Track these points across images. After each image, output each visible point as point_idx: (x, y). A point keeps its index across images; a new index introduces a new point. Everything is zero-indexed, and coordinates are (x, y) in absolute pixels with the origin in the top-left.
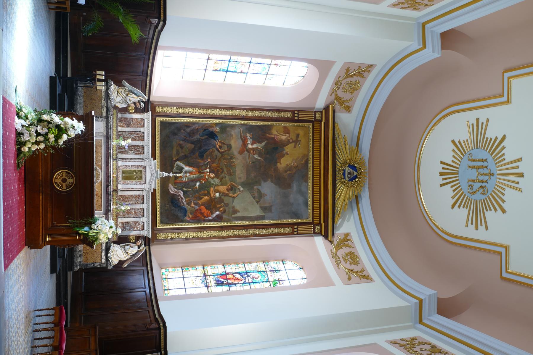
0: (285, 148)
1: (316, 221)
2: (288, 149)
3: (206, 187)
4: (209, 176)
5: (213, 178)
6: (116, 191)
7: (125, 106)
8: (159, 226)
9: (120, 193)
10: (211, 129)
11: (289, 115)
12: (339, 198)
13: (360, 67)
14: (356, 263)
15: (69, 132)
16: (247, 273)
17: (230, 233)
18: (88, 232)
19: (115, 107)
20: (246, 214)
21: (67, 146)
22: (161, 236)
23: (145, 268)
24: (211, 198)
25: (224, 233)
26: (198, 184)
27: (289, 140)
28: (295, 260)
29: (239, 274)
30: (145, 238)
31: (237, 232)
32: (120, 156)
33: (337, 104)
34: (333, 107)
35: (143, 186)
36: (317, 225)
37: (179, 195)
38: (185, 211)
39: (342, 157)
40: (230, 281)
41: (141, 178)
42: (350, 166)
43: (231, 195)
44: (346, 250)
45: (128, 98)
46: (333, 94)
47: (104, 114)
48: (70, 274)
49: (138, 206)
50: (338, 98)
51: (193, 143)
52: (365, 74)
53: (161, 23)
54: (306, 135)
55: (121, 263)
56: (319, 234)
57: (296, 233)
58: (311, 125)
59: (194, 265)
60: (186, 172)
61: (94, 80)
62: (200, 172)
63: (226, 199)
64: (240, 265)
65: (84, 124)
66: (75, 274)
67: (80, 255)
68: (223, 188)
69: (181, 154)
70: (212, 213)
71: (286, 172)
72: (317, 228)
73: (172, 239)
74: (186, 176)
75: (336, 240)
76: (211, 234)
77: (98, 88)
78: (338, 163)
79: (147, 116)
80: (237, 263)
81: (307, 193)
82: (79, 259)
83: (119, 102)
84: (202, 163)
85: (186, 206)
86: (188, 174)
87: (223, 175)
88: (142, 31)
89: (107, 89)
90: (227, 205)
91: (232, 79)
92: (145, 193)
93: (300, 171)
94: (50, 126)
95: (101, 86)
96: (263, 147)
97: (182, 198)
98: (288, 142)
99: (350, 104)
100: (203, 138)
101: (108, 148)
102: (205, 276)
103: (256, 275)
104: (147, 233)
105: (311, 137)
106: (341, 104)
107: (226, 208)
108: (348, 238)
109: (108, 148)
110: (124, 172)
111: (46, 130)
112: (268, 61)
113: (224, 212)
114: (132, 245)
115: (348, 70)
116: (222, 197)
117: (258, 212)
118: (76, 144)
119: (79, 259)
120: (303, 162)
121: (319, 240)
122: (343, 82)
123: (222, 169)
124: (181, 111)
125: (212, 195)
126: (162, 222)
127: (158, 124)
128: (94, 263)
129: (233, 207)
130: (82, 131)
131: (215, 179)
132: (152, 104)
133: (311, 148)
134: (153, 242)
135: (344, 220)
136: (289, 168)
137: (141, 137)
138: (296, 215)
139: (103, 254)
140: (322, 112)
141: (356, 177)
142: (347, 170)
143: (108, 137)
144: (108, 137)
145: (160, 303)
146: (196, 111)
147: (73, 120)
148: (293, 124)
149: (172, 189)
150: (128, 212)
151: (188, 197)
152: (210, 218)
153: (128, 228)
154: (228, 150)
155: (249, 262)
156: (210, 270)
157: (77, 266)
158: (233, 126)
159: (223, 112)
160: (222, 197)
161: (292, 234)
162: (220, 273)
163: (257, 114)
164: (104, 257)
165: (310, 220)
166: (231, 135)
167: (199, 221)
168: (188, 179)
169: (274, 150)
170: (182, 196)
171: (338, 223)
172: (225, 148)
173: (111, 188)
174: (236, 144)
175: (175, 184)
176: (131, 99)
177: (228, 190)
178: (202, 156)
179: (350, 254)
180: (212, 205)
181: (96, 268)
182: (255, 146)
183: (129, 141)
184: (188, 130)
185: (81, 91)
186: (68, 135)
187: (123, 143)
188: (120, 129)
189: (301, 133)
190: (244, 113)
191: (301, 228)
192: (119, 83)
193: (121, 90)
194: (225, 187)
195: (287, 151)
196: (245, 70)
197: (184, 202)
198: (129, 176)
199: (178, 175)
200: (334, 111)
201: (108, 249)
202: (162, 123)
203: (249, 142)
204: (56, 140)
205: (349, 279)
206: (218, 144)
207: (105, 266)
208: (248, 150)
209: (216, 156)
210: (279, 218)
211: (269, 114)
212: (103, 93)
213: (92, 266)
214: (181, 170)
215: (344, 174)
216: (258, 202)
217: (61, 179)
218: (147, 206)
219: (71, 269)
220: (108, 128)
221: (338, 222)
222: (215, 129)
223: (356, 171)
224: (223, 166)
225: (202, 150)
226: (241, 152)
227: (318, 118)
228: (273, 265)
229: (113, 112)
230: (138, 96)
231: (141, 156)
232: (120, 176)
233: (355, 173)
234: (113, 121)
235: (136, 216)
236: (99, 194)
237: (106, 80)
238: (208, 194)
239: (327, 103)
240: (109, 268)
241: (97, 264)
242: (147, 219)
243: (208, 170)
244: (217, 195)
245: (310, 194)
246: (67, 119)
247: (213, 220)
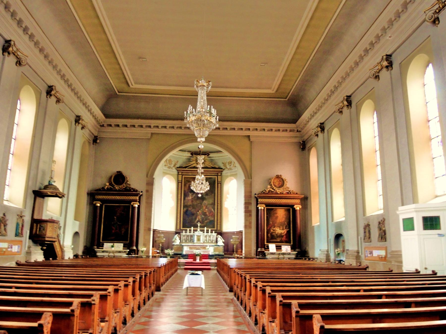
1: (216, 174)
11: (180, 184)
22: (219, 229)
44: (227, 164)
50: (174, 166)
55: (223, 242)
56: (221, 173)
58: (183, 176)
75: (223, 167)
202: (183, 227)
210: (215, 188)
244: (206, 209)
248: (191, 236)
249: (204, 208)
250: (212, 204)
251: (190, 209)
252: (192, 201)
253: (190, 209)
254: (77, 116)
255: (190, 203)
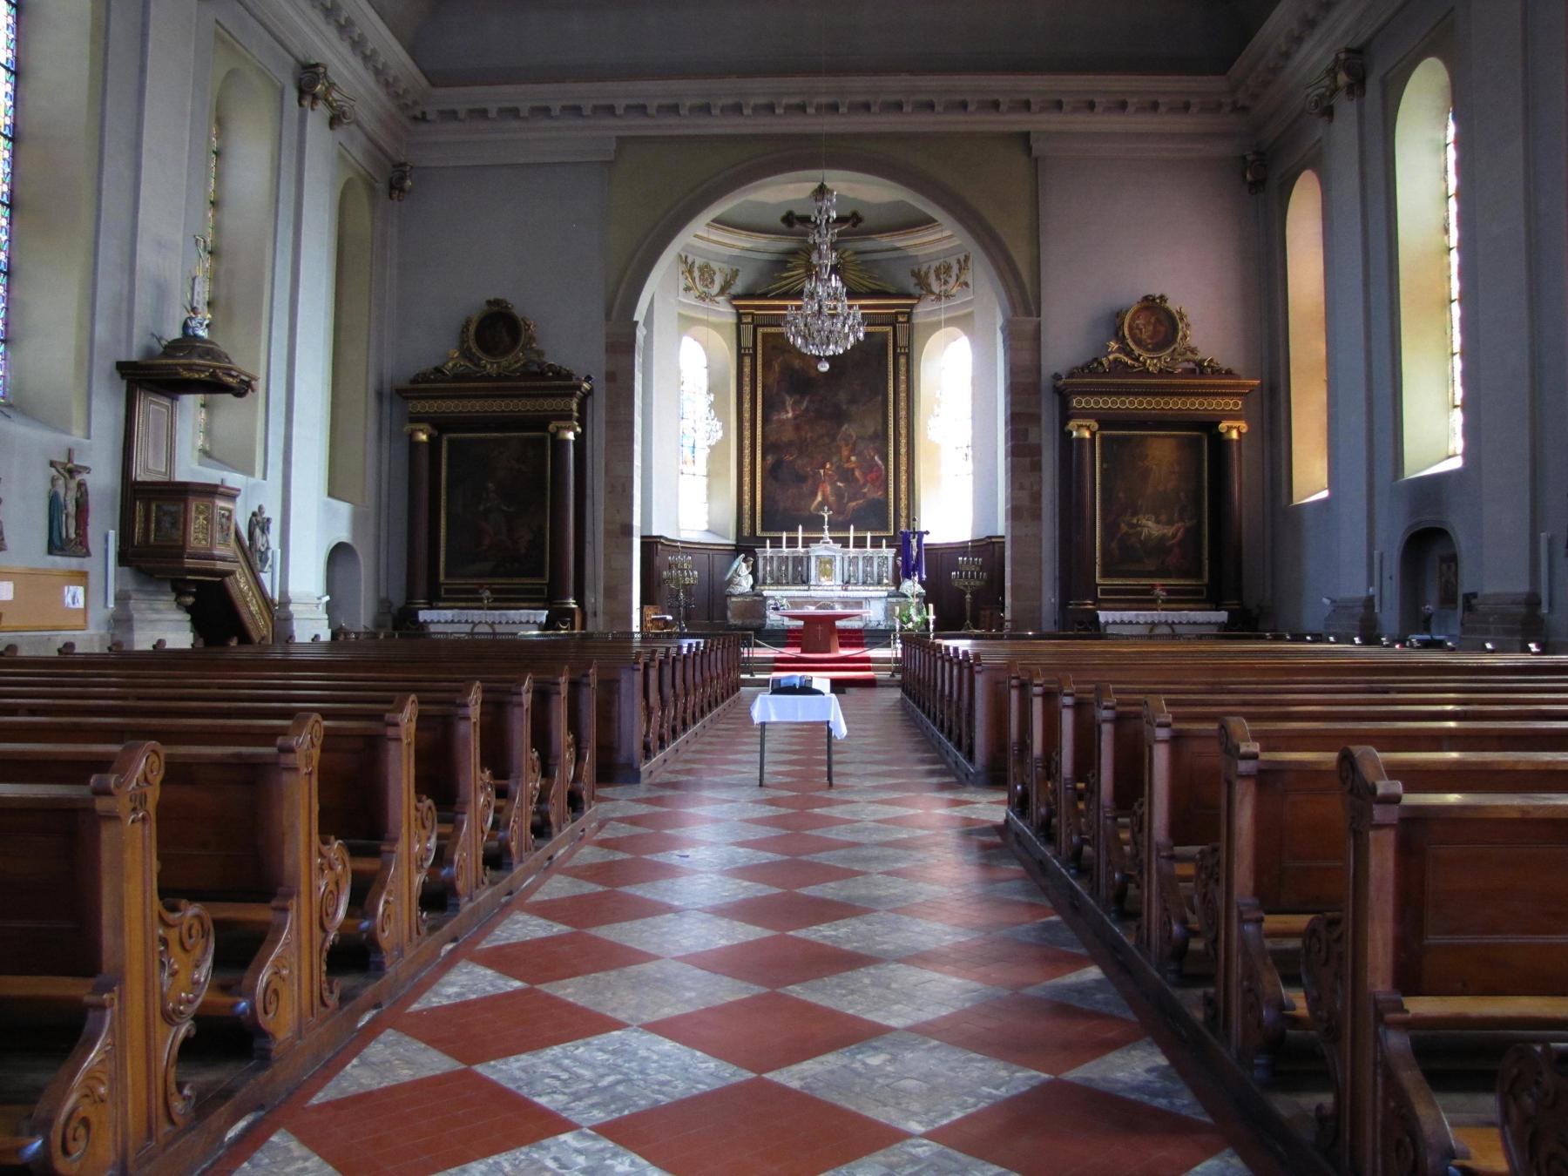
11: (747, 361)
14: (948, 268)
50: (722, 291)
56: (910, 315)
58: (760, 330)
75: (915, 291)
161: (909, 357)
248: (798, 561)
249: (845, 453)
250: (875, 437)
251: (788, 458)
252: (797, 428)
253: (788, 458)
254: (399, 166)
255: (788, 435)
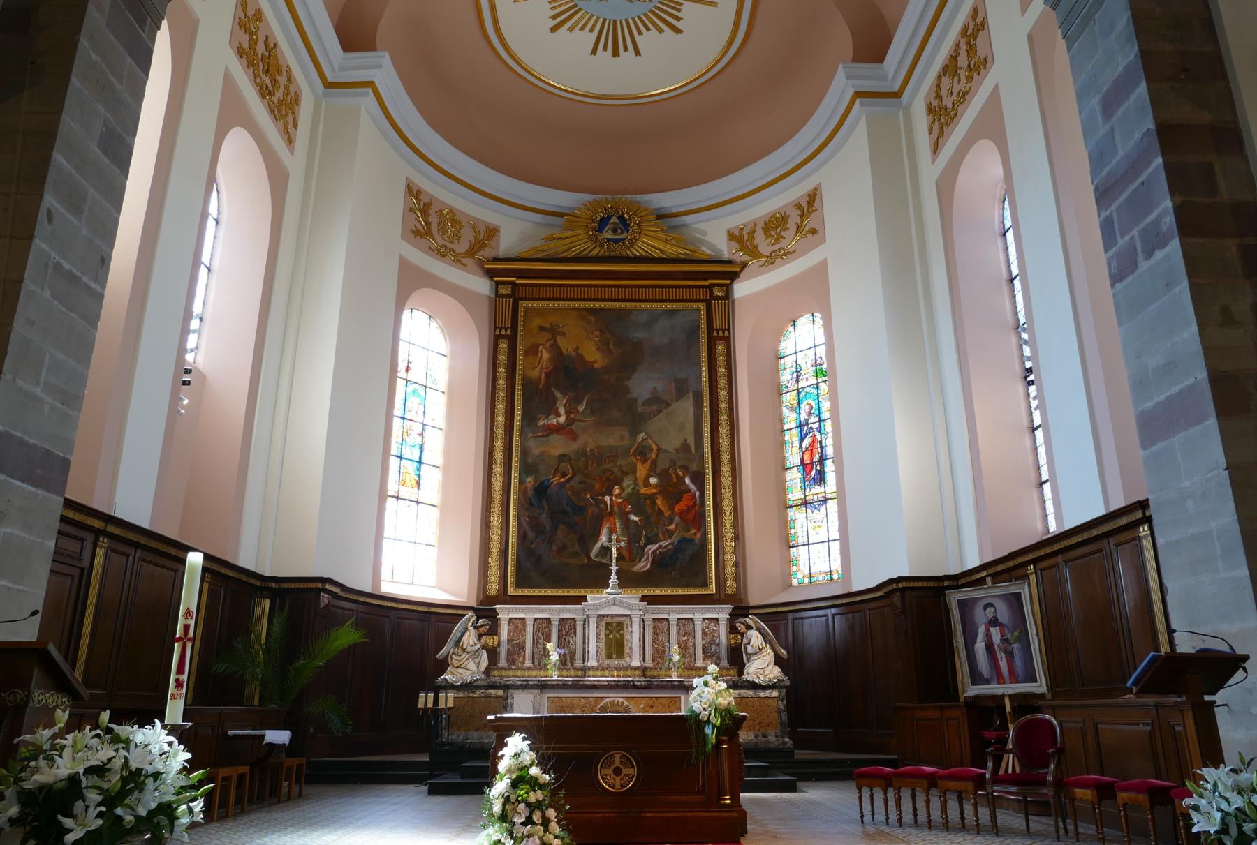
0: (565, 352)
1: (704, 294)
2: (567, 346)
3: (637, 501)
4: (618, 496)
5: (622, 489)
6: (644, 670)
7: (484, 654)
8: (713, 589)
9: (649, 664)
10: (530, 493)
11: (503, 345)
12: (662, 251)
13: (411, 210)
15: (527, 763)
16: (801, 426)
17: (725, 457)
18: (714, 726)
19: (487, 672)
20: (690, 427)
21: (552, 767)
23: (790, 616)
24: (659, 493)
25: (726, 469)
26: (634, 518)
27: (551, 346)
28: (778, 335)
29: (802, 439)
30: (734, 616)
31: (724, 444)
32: (578, 664)
33: (482, 253)
34: (488, 261)
35: (636, 621)
36: (711, 293)
37: (654, 552)
38: (684, 541)
39: (582, 245)
40: (817, 457)
41: (620, 624)
42: (600, 230)
43: (653, 456)
44: (759, 237)
45: (469, 649)
46: (464, 260)
47: (500, 692)
48: (800, 754)
49: (673, 630)
50: (471, 252)
51: (556, 528)
52: (425, 199)
53: (328, 587)
54: (540, 313)
55: (779, 661)
56: (728, 290)
57: (726, 334)
59: (785, 524)
60: (610, 540)
61: (436, 712)
62: (611, 514)
63: (662, 465)
64: (787, 438)
65: (510, 736)
66: (798, 744)
67: (765, 736)
68: (642, 471)
69: (577, 548)
70: (689, 491)
71: (610, 351)
72: (717, 292)
73: (736, 565)
74: (618, 541)
75: (740, 257)
76: (727, 493)
77: (450, 704)
78: (594, 253)
79: (505, 612)
80: (781, 445)
81: (651, 311)
82: (772, 739)
83: (478, 665)
84: (593, 510)
85: (675, 538)
86: (614, 537)
87: (615, 470)
88: (342, 624)
89: (452, 687)
90: (673, 463)
91: (435, 454)
92: (649, 617)
93: (609, 325)
94: (513, 798)
95: (448, 699)
96: (565, 395)
97: (660, 547)
98: (555, 349)
99: (482, 229)
100: (546, 506)
101: (563, 686)
102: (805, 503)
103: (804, 408)
104: (723, 612)
105: (545, 304)
106: (482, 246)
107: (679, 464)
108: (737, 233)
109: (563, 686)
110: (609, 657)
111: (522, 806)
112: (400, 384)
113: (685, 468)
114: (745, 641)
115: (416, 233)
116: (658, 471)
117: (687, 405)
118: (548, 749)
119: (772, 739)
120: (592, 318)
121: (741, 289)
122: (441, 242)
123: (605, 472)
124: (495, 549)
125: (654, 491)
126: (705, 584)
127: (520, 593)
128: (779, 711)
129: (677, 451)
130: (524, 739)
131: (625, 484)
132: (481, 602)
133: (566, 304)
134: (741, 601)
135: (702, 242)
136: (604, 347)
137: (543, 626)
138: (693, 332)
139: (762, 695)
140: (498, 283)
141: (621, 218)
142: (607, 234)
143: (543, 686)
144: (543, 686)
145: (856, 588)
146: (496, 520)
147: (502, 756)
148: (520, 338)
149: (643, 565)
150: (685, 648)
151: (657, 535)
152: (697, 494)
153: (714, 647)
154: (570, 460)
155: (781, 421)
156: (795, 495)
157: (785, 743)
158: (524, 452)
159: (498, 469)
160: (658, 471)
161: (728, 341)
162: (799, 475)
163: (501, 407)
164: (768, 693)
165: (702, 306)
166: (542, 454)
167: (703, 515)
168: (623, 535)
169: (569, 375)
170: (655, 547)
171: (709, 252)
172: (565, 466)
173: (638, 679)
174: (558, 446)
175: (633, 560)
176: (471, 642)
177: (644, 461)
178: (581, 510)
179: (767, 229)
180: (672, 491)
181: (788, 708)
182: (562, 410)
183: (550, 646)
184: (531, 535)
185: (457, 736)
186: (531, 765)
187: (554, 657)
188: (528, 664)
189: (537, 322)
190: (499, 431)
191: (717, 324)
192: (443, 665)
193: (455, 661)
194: (639, 466)
195: (570, 349)
196: (419, 428)
197: (667, 543)
198: (615, 645)
199: (614, 556)
200: (496, 260)
201: (754, 686)
202: (519, 585)
203: (554, 421)
204: (542, 787)
205: (814, 232)
206: (557, 479)
207: (784, 692)
208: (570, 422)
209: (581, 482)
210: (699, 364)
211: (502, 382)
212: (461, 695)
213: (784, 715)
214: (606, 551)
215: (616, 241)
216: (668, 405)
217: (617, 776)
218: (673, 613)
219: (790, 753)
220: (525, 687)
221: (706, 251)
222: (529, 485)
223: (610, 217)
224: (599, 471)
225: (568, 509)
226: (574, 436)
227: (508, 291)
228: (786, 377)
229: (496, 676)
230: (467, 629)
231: (579, 624)
232: (616, 663)
233: (613, 220)
234: (513, 676)
235: (691, 633)
236: (650, 702)
237: (437, 690)
238: (652, 497)
239: (481, 272)
240: (788, 683)
241: (781, 705)
242: (698, 613)
243: (607, 498)
244: (653, 481)
245: (653, 305)
246: (502, 766)
247: (702, 489)
